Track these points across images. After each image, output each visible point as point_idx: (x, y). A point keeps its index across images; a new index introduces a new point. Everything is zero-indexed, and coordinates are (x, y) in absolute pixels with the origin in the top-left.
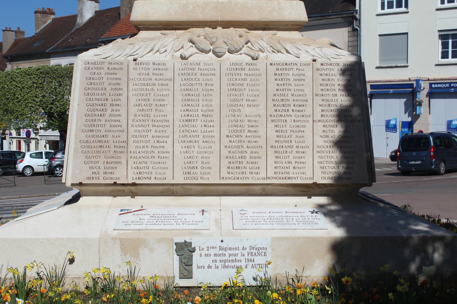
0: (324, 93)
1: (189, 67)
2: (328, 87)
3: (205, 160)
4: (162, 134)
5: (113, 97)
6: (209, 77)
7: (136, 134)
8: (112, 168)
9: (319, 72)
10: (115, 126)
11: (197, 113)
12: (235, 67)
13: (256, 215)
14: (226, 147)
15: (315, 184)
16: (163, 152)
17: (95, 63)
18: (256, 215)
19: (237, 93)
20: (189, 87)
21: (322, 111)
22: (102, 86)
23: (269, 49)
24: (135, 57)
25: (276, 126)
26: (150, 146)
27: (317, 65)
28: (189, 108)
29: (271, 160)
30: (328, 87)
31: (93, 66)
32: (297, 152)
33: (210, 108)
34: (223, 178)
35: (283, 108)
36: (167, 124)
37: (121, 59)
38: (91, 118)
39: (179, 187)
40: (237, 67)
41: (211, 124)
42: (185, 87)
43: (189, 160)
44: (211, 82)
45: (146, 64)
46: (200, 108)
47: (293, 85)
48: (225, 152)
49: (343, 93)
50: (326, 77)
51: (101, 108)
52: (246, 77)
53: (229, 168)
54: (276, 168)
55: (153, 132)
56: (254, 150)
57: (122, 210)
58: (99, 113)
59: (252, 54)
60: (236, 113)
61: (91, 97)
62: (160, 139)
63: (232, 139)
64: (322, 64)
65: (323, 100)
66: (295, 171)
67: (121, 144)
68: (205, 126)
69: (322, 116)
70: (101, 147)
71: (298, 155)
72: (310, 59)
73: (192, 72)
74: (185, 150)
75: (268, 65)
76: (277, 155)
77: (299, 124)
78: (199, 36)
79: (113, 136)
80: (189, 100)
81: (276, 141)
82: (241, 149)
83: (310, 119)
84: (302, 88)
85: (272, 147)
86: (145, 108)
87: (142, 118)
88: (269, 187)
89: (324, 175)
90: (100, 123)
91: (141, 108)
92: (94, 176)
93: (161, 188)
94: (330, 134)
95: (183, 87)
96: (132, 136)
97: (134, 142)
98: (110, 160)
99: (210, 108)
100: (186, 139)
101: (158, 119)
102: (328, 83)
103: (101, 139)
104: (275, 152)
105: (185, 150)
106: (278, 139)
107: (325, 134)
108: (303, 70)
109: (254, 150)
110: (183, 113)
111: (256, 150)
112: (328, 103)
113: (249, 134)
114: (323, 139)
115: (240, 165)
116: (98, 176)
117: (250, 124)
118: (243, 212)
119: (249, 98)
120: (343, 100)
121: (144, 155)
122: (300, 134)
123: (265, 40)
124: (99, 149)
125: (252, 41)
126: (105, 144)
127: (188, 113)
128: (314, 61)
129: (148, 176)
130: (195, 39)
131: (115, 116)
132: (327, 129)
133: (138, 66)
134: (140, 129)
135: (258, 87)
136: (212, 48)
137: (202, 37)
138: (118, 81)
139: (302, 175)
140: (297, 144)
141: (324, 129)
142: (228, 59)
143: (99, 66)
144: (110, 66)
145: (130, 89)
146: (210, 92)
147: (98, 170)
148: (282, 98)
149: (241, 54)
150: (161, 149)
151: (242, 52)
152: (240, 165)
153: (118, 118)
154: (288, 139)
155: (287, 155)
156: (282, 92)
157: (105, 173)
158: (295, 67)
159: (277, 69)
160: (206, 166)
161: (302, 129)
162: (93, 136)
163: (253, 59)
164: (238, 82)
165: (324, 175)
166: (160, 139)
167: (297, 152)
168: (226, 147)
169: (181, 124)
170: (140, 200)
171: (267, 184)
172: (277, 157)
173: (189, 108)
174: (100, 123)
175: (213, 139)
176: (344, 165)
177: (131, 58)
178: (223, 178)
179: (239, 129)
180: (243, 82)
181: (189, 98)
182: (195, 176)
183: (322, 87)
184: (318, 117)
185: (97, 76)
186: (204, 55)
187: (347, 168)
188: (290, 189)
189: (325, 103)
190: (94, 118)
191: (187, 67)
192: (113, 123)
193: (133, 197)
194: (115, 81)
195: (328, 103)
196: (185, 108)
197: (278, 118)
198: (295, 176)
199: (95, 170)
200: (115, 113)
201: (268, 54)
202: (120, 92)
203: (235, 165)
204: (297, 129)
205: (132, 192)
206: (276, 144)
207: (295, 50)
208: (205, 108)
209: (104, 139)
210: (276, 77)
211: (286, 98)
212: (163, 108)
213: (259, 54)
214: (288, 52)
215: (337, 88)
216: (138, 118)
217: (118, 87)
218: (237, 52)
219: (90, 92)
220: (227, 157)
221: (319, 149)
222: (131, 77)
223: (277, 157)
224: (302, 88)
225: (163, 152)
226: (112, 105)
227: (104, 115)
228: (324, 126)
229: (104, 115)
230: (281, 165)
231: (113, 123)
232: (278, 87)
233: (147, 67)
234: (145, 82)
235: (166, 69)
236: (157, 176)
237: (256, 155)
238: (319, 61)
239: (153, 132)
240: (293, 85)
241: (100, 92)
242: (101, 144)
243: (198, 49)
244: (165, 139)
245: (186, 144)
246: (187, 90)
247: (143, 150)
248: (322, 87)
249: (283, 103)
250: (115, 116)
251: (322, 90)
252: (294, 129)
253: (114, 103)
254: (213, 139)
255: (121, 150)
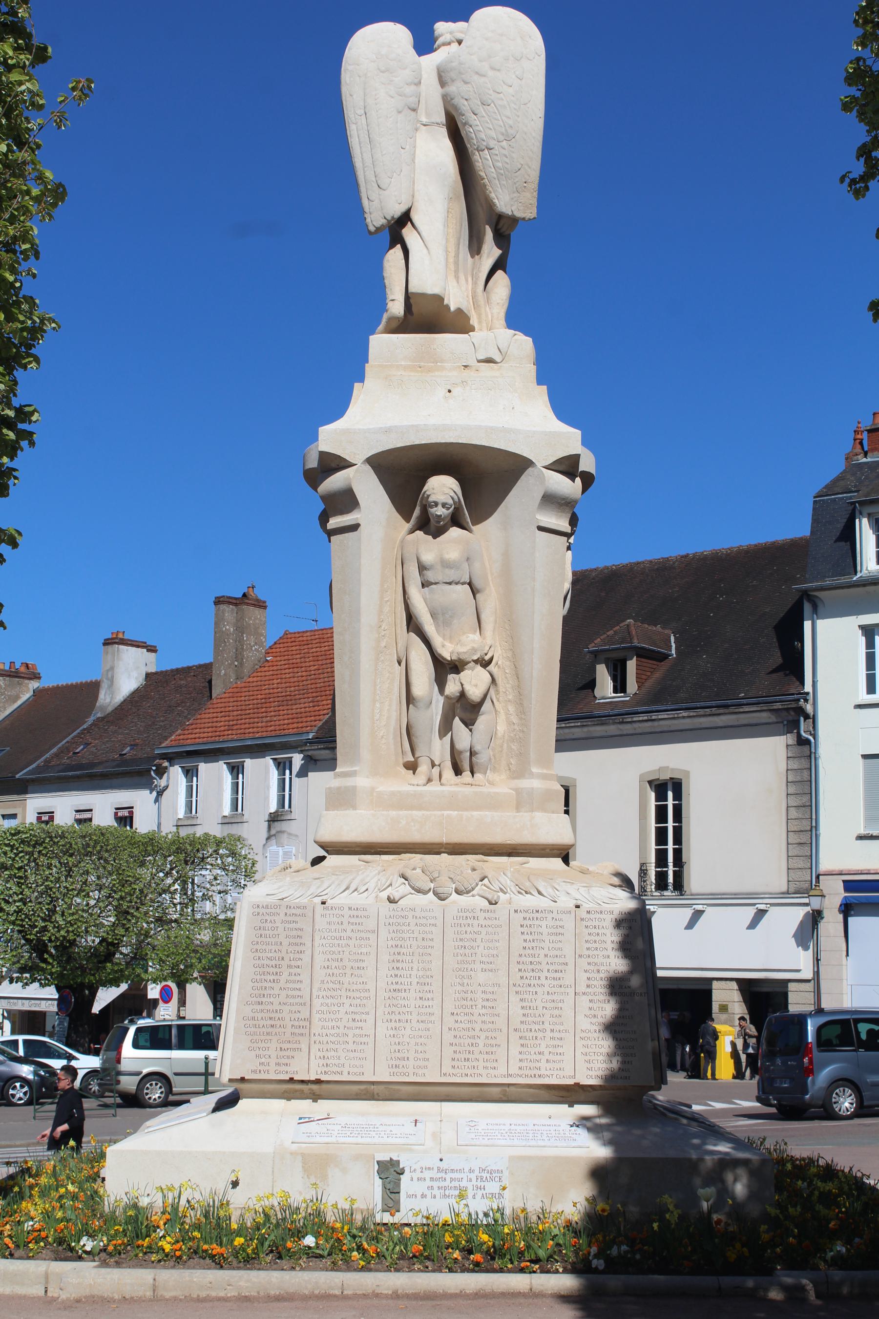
0: (590, 953)
1: (399, 913)
2: (597, 945)
3: (420, 1048)
4: (359, 1009)
5: (292, 956)
6: (427, 929)
7: (322, 1008)
8: (288, 1057)
9: (584, 923)
10: (294, 997)
11: (409, 980)
12: (465, 915)
13: (490, 1127)
14: (450, 1029)
15: (577, 1084)
16: (361, 1036)
17: (267, 907)
18: (490, 1127)
19: (467, 951)
20: (399, 943)
21: (588, 979)
22: (276, 940)
23: (513, 889)
24: (324, 898)
25: (521, 1000)
26: (342, 1027)
27: (582, 912)
28: (399, 973)
29: (514, 1050)
30: (597, 945)
31: (264, 911)
32: (552, 1038)
33: (428, 973)
34: (445, 1075)
35: (532, 974)
36: (366, 994)
37: (304, 901)
38: (260, 985)
39: (382, 1087)
40: (468, 914)
41: (429, 995)
42: (394, 943)
43: (397, 1047)
44: (430, 936)
45: (340, 908)
46: (414, 973)
47: (547, 941)
48: (448, 1037)
49: (619, 954)
50: (594, 931)
51: (275, 970)
52: (480, 929)
53: (453, 1059)
54: (521, 1060)
55: (347, 1006)
56: (489, 1034)
57: (300, 1119)
58: (272, 978)
59: (490, 897)
60: (466, 981)
61: (261, 955)
62: (357, 1017)
63: (459, 1018)
64: (588, 912)
65: (589, 964)
66: (549, 1065)
67: (302, 1023)
68: (421, 998)
69: (588, 986)
70: (272, 1026)
71: (553, 1042)
72: (571, 905)
73: (404, 920)
74: (392, 1032)
75: (512, 912)
76: (522, 1041)
77: (555, 997)
78: (414, 869)
79: (290, 1011)
80: (398, 961)
81: (522, 1022)
82: (471, 1033)
83: (571, 991)
84: (559, 945)
85: (515, 1030)
86: (336, 971)
87: (331, 985)
88: (512, 1089)
89: (591, 1073)
90: (272, 992)
91: (330, 971)
92: (261, 1068)
93: (355, 1088)
94: (600, 1013)
95: (390, 943)
96: (318, 1012)
97: (320, 1020)
98: (285, 1046)
99: (428, 973)
100: (393, 1017)
101: (355, 987)
102: (597, 938)
103: (273, 1015)
104: (521, 1038)
105: (392, 1032)
106: (524, 1019)
107: (592, 1012)
108: (561, 920)
109: (489, 1034)
110: (390, 980)
111: (494, 1034)
112: (596, 968)
113: (484, 1011)
114: (589, 1020)
115: (470, 1056)
116: (267, 1068)
117: (485, 996)
118: (473, 1124)
119: (483, 959)
120: (618, 964)
121: (333, 1039)
122: (556, 1012)
123: (509, 875)
124: (270, 1030)
125: (490, 876)
126: (278, 1023)
127: (397, 979)
128: (578, 907)
129: (339, 1070)
130: (409, 873)
131: (294, 982)
132: (595, 1006)
133: (328, 912)
134: (329, 1001)
135: (497, 944)
136: (432, 885)
137: (419, 871)
138: (299, 933)
139: (559, 1072)
140: (552, 1027)
141: (591, 1005)
142: (454, 902)
143: (273, 911)
144: (289, 911)
145: (316, 944)
146: (429, 951)
147: (268, 1060)
148: (531, 959)
149: (473, 896)
150: (357, 1032)
151: (474, 892)
152: (470, 1056)
153: (297, 986)
154: (538, 1019)
155: (537, 1042)
156: (531, 952)
157: (278, 1064)
158: (550, 916)
159: (525, 919)
160: (420, 1056)
161: (560, 1005)
162: (262, 1011)
163: (491, 903)
164: (468, 936)
165: (591, 1073)
166: (357, 1017)
167: (552, 1038)
168: (450, 1029)
169: (387, 995)
170: (325, 1106)
171: (509, 1085)
172: (522, 1045)
173: (399, 973)
174: (272, 992)
175: (432, 1018)
176: (619, 1058)
177: (318, 900)
178: (445, 1075)
179: (469, 1003)
180: (476, 936)
181: (399, 958)
182: (405, 1070)
183: (589, 945)
184: (582, 988)
185: (270, 925)
186: (421, 896)
187: (623, 1062)
188: (543, 1093)
189: (592, 967)
190: (265, 984)
191: (396, 913)
192: (290, 993)
193: (315, 1101)
194: (295, 933)
195: (596, 968)
196: (393, 972)
197: (524, 989)
198: (548, 1073)
199: (263, 1060)
200: (293, 978)
201: (513, 895)
202: (302, 948)
203: (463, 1056)
204: (552, 1005)
205: (314, 1094)
206: (523, 1027)
207: (550, 890)
208: (421, 973)
209: (277, 1015)
210: (522, 930)
211: (537, 960)
212: (361, 972)
213: (499, 897)
214: (540, 893)
215: (610, 949)
216: (326, 986)
217: (298, 941)
218: (468, 892)
219: (259, 947)
220: (451, 1044)
221: (583, 1035)
222: (317, 927)
223: (522, 1045)
224: (559, 945)
225: (361, 1036)
226: (289, 966)
227: (278, 981)
228: (591, 1001)
229: (278, 981)
230: (529, 1057)
231: (290, 993)
232: (525, 944)
233: (340, 912)
234: (338, 935)
235: (367, 917)
236: (352, 1070)
237: (493, 1042)
238: (585, 906)
239: (347, 1006)
240: (547, 941)
241: (274, 948)
242: (273, 1022)
243: (413, 888)
244: (364, 1017)
245: (393, 1024)
246: (396, 946)
247: (333, 1032)
248: (589, 945)
249: (533, 967)
250: (294, 982)
251: (588, 949)
252: (548, 1005)
253: (293, 963)
254: (432, 1018)
255: (301, 1031)
